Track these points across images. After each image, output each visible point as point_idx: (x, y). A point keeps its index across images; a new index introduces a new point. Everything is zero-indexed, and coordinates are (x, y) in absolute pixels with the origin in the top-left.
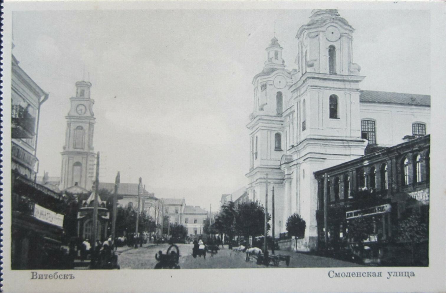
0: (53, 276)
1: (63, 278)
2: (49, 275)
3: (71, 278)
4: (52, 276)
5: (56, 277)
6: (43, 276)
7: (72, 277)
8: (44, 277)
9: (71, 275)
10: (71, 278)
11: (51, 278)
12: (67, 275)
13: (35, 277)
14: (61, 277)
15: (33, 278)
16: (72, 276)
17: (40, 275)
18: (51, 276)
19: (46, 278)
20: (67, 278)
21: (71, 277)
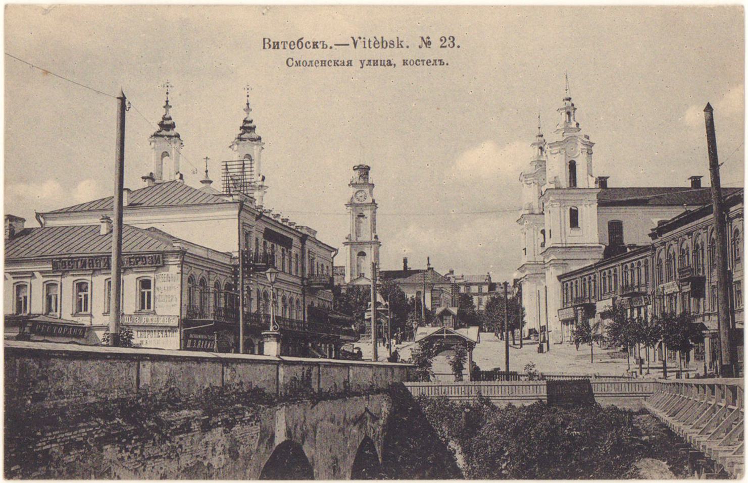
0: (296, 43)
1: (312, 47)
2: (289, 43)
3: (323, 48)
4: (294, 44)
5: (300, 43)
6: (280, 44)
7: (325, 46)
8: (281, 46)
9: (323, 42)
10: (323, 48)
11: (292, 47)
12: (317, 42)
13: (267, 46)
14: (308, 46)
15: (264, 48)
16: (325, 43)
17: (274, 43)
18: (292, 43)
19: (284, 48)
20: (317, 47)
21: (323, 45)
